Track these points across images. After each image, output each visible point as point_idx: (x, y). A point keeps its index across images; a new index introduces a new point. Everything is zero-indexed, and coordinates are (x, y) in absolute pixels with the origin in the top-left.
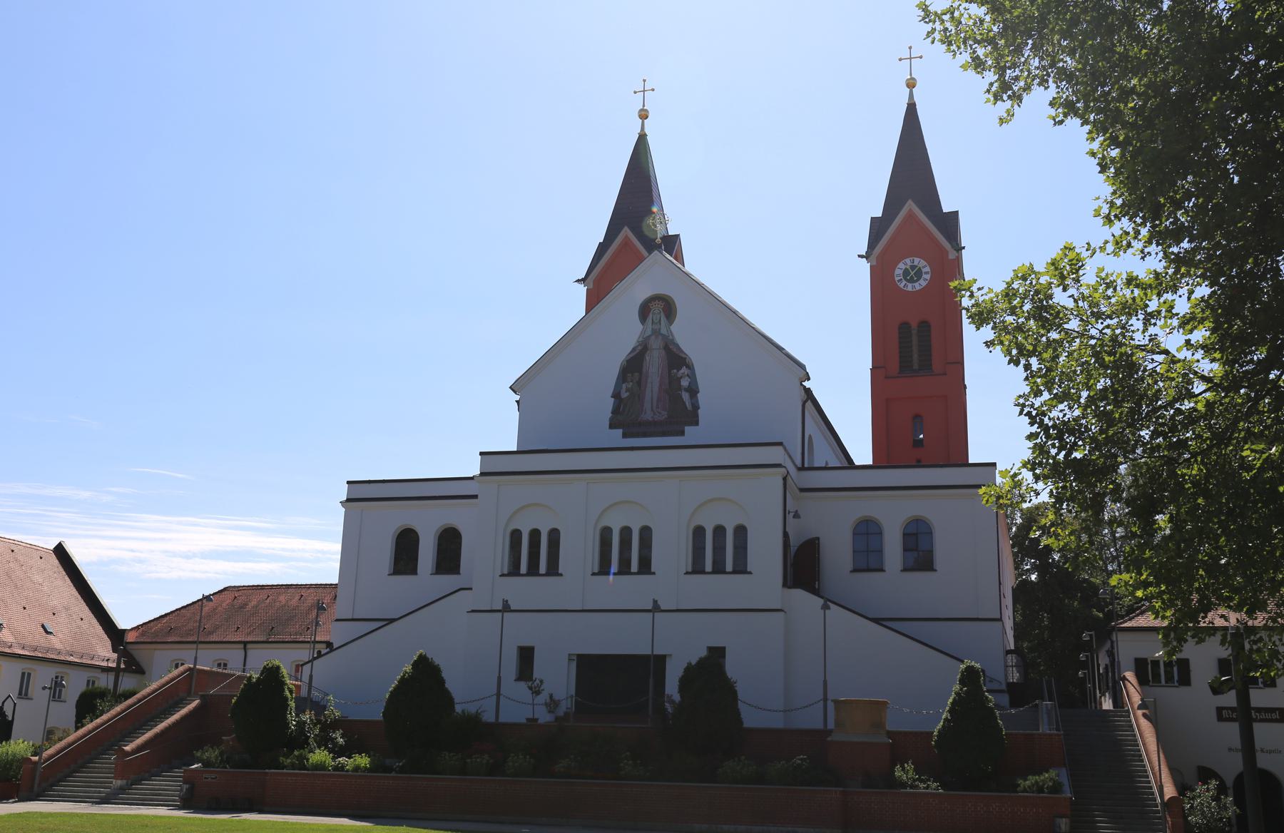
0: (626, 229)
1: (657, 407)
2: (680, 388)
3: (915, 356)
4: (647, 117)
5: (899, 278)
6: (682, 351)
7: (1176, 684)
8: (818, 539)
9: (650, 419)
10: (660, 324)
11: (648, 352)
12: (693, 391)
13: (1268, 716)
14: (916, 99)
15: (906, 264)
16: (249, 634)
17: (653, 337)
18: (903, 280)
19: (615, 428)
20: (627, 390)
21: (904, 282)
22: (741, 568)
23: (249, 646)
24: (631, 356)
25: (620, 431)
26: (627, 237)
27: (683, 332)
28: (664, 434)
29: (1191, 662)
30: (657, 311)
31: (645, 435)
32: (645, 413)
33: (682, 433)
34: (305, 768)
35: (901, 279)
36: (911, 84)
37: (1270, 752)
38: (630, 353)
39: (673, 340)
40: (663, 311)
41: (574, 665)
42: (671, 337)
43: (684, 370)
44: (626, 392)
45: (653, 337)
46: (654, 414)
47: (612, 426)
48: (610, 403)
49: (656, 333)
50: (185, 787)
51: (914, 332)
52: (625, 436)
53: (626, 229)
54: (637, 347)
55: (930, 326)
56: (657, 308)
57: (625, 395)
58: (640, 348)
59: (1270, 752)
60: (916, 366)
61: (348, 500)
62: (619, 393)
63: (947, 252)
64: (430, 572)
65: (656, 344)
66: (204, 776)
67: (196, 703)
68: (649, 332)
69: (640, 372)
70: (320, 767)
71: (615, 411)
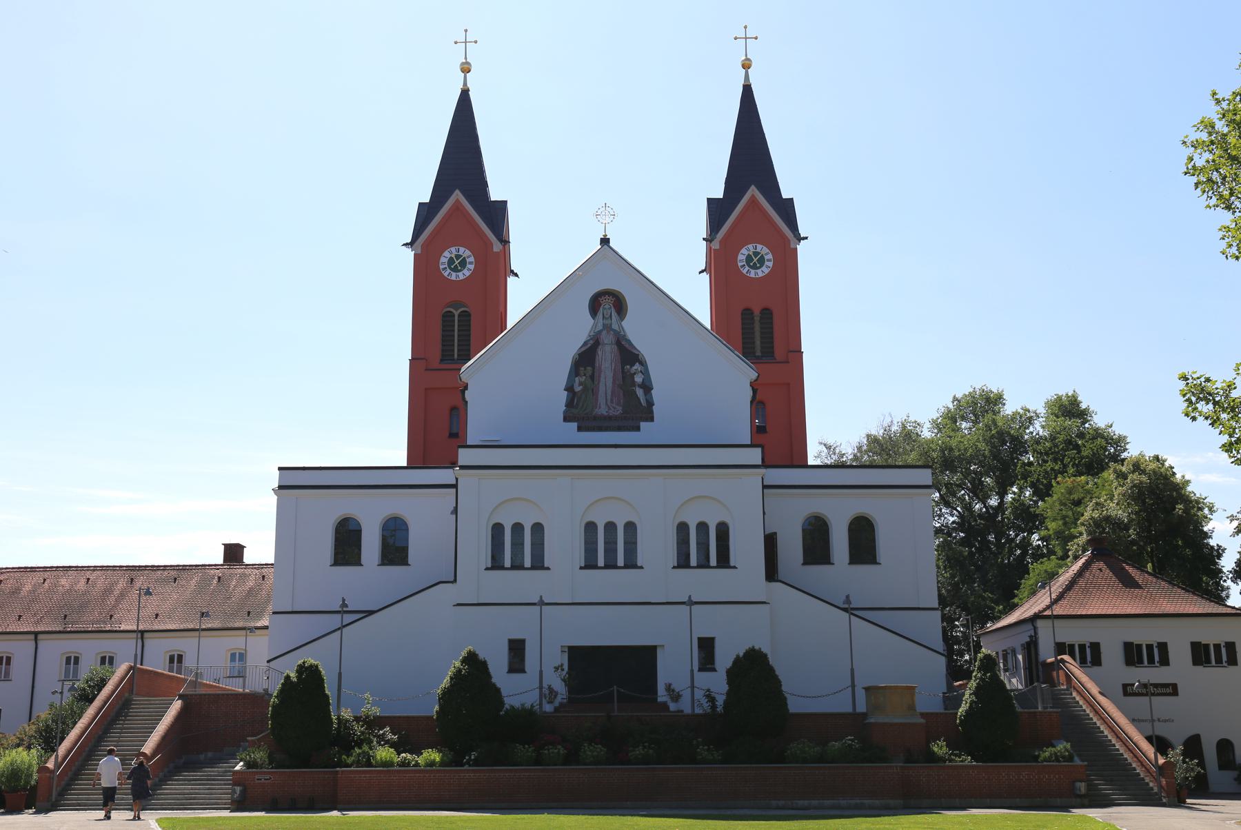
1: (612, 402)
2: (633, 383)
3: (758, 343)
4: (468, 72)
5: (743, 264)
6: (636, 349)
7: (1089, 664)
8: (775, 533)
9: (606, 414)
10: (611, 320)
11: (600, 347)
12: (647, 387)
13: (1164, 691)
14: (752, 81)
15: (749, 250)
16: (38, 623)
17: (604, 332)
18: (746, 266)
19: (569, 421)
20: (580, 384)
21: (747, 268)
22: (724, 560)
23: (40, 637)
24: (583, 349)
25: (574, 425)
27: (635, 328)
28: (619, 429)
29: (1101, 644)
30: (607, 306)
31: (600, 429)
32: (600, 408)
33: (638, 429)
34: (369, 764)
35: (744, 265)
36: (746, 65)
37: (1166, 721)
38: (581, 347)
39: (625, 335)
40: (614, 306)
41: (566, 655)
42: (622, 333)
43: (637, 366)
44: (579, 385)
45: (604, 332)
46: (609, 409)
47: (566, 419)
48: (563, 396)
49: (608, 327)
50: (238, 789)
51: (757, 319)
52: (580, 429)
53: (457, 192)
54: (589, 340)
55: (771, 314)
56: (607, 305)
57: (578, 388)
58: (591, 342)
59: (1166, 721)
60: (758, 353)
61: (280, 487)
62: (573, 386)
63: (789, 240)
64: (377, 563)
65: (607, 339)
66: (256, 777)
67: (177, 705)
68: (600, 327)
69: (593, 367)
70: (387, 764)
71: (569, 404)
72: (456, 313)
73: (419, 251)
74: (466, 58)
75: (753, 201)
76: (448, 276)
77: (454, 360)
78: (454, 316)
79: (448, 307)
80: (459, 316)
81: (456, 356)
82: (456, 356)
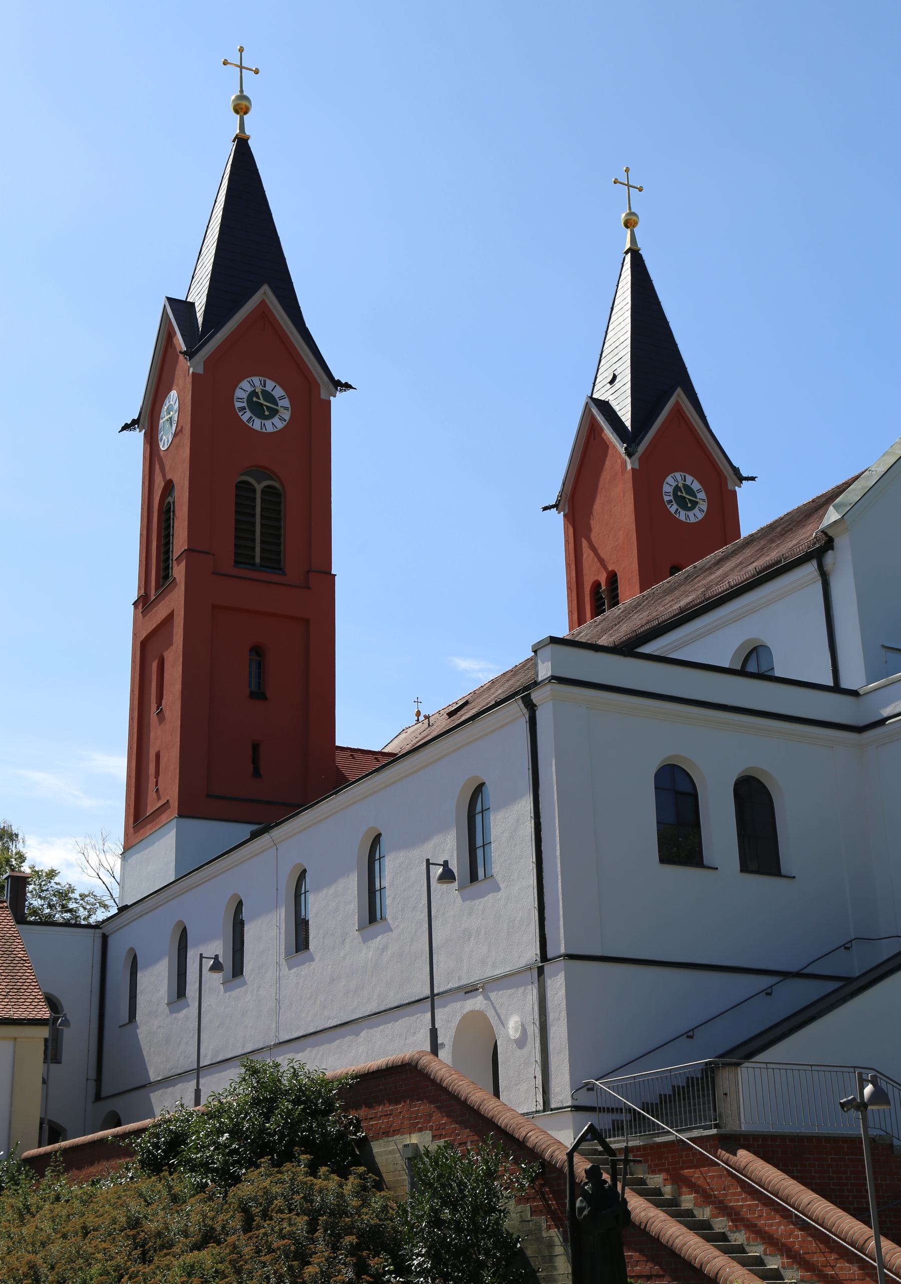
0: (265, 288)
4: (246, 113)
26: (263, 303)
53: (265, 288)
72: (259, 488)
73: (200, 370)
74: (242, 91)
75: (678, 410)
76: (249, 420)
77: (254, 565)
78: (254, 490)
79: (244, 474)
80: (263, 491)
81: (258, 560)
82: (258, 560)
